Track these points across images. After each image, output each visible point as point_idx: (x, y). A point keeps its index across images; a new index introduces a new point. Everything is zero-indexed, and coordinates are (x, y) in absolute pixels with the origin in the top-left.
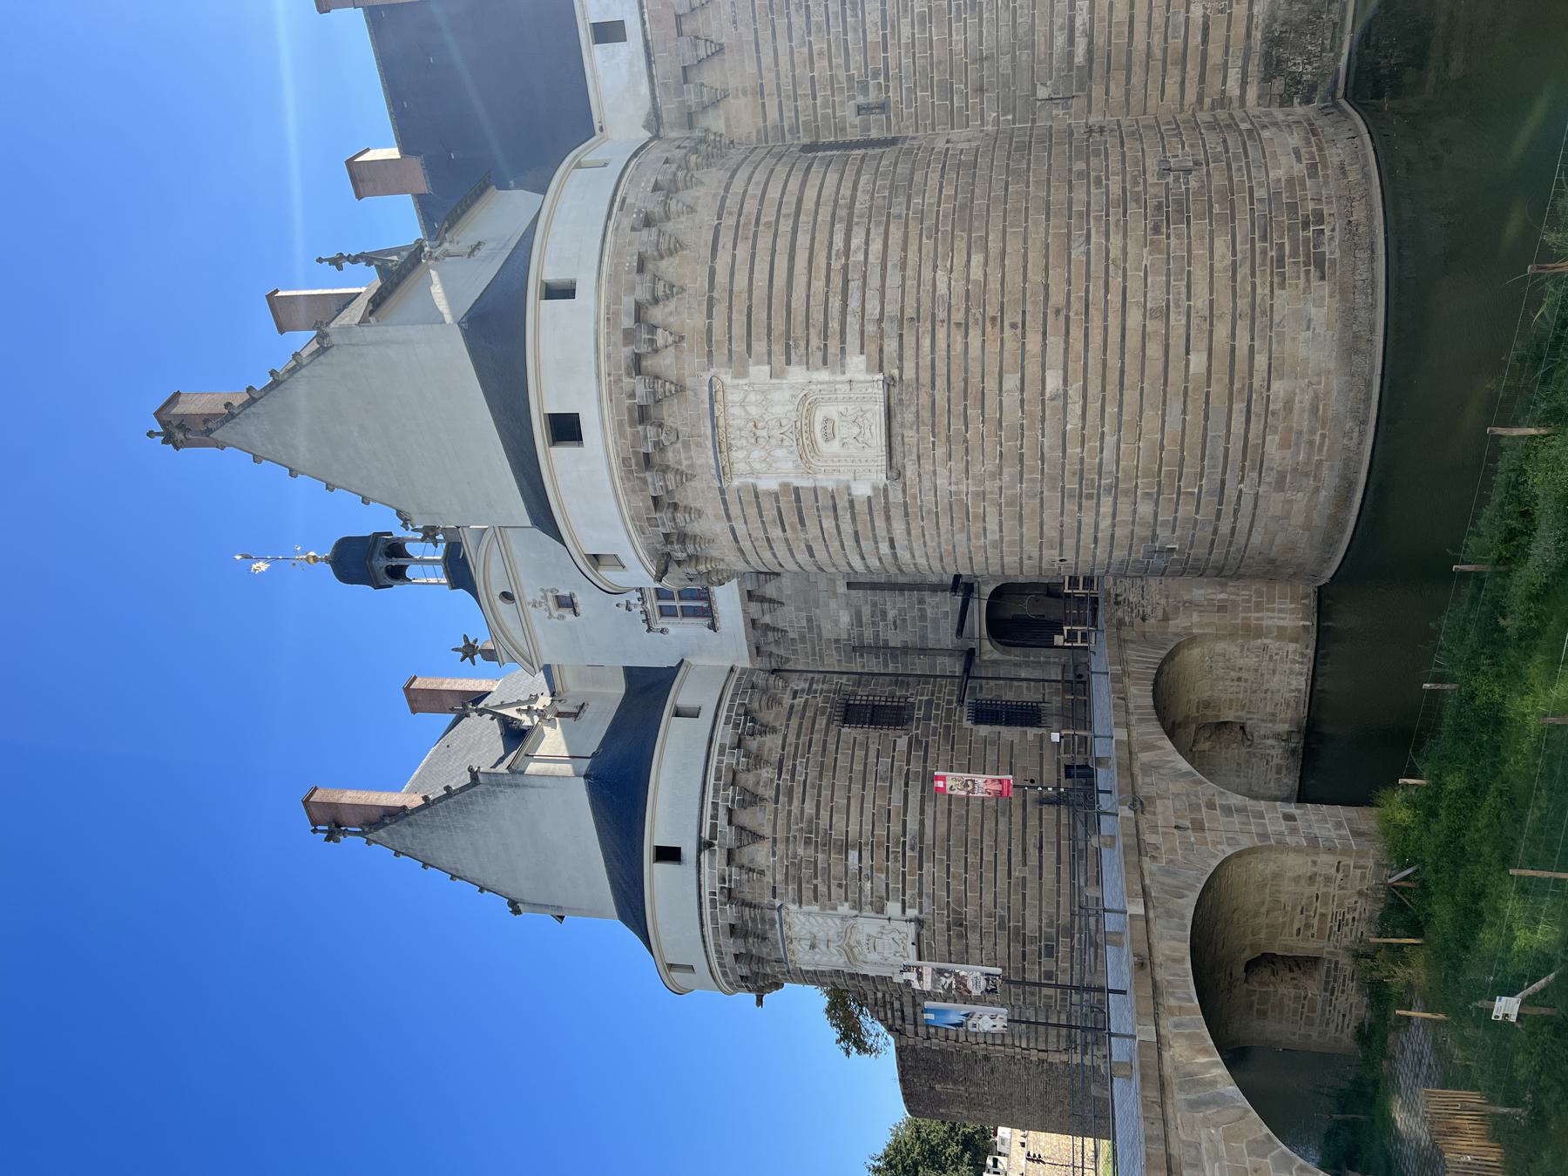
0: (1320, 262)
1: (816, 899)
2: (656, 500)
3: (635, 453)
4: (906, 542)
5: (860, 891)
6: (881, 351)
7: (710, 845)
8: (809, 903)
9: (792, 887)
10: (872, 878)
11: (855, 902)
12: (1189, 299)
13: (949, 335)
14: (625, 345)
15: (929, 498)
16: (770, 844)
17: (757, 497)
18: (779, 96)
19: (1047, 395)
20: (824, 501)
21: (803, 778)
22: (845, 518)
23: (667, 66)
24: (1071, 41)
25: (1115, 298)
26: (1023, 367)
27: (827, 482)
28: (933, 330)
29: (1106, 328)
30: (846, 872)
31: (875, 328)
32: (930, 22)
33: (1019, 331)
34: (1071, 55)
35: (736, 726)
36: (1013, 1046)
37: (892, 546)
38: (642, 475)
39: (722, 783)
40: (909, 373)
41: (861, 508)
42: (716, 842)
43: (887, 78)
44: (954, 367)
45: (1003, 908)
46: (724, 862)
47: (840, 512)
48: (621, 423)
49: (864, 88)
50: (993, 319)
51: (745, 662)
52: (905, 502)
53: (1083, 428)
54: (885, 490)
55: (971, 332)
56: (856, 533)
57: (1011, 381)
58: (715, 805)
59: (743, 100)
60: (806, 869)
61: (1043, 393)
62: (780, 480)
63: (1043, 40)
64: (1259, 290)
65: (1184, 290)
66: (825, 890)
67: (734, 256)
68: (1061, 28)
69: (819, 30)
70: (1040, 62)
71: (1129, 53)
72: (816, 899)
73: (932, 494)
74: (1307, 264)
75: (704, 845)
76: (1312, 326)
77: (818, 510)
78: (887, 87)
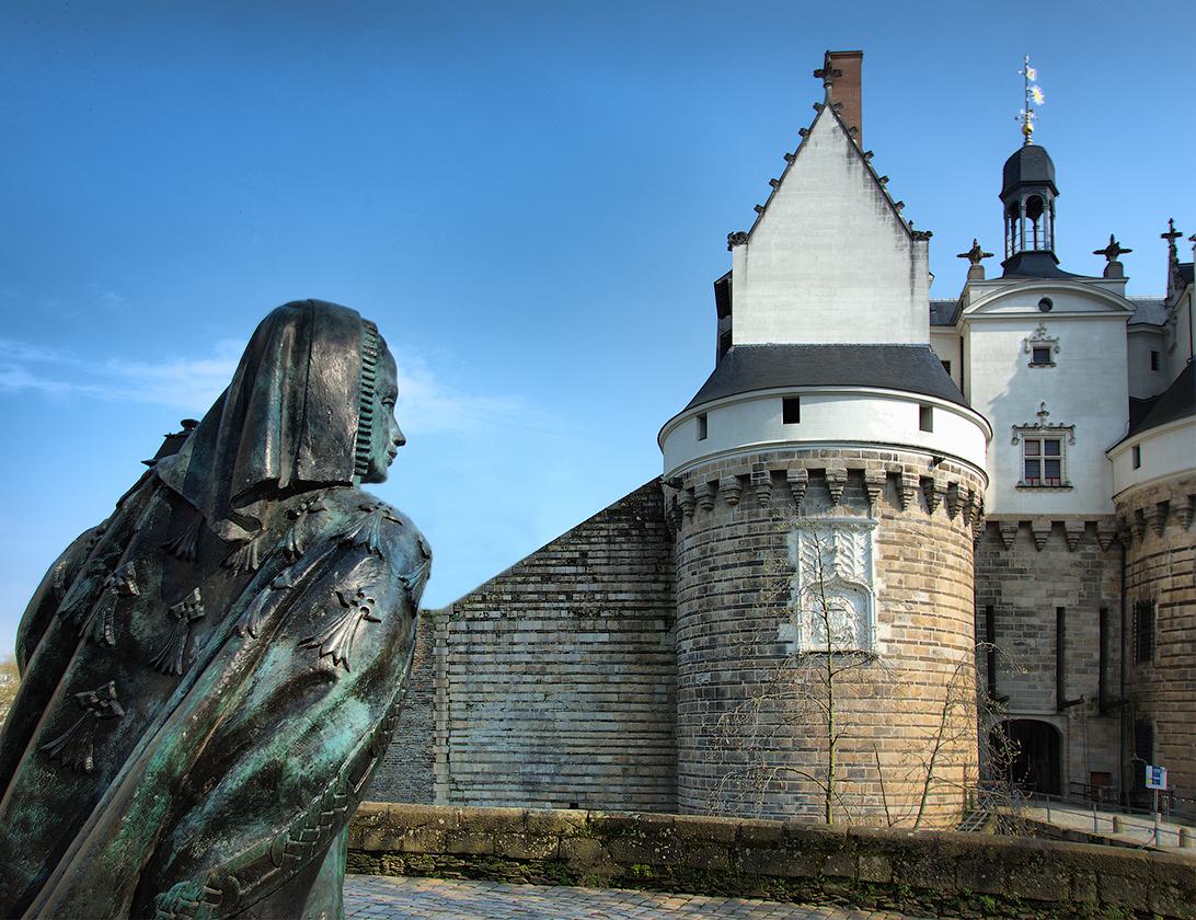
1: (885, 557)
8: (881, 551)
9: (895, 536)
11: (887, 595)
36: (450, 730)
45: (896, 732)
66: (896, 568)
72: (885, 557)
75: (937, 459)
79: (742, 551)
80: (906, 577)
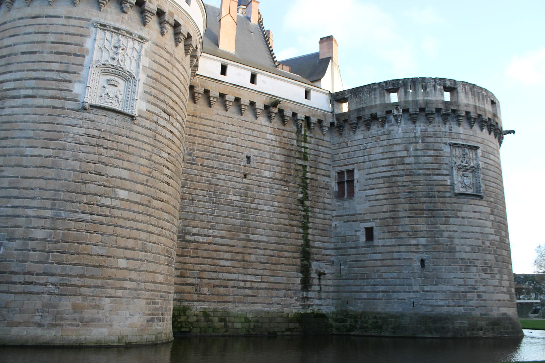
0: (152, 320)
4: (30, 104)
6: (147, 119)
12: (147, 261)
13: (148, 151)
14: (169, 11)
15: (66, 121)
17: (81, 35)
18: (191, 122)
19: (117, 190)
20: (72, 68)
23: (210, 86)
24: (194, 235)
25: (151, 228)
26: (131, 181)
27: (83, 73)
28: (150, 145)
29: (141, 222)
31: (155, 120)
32: (208, 184)
33: (145, 183)
34: (189, 234)
37: (26, 97)
40: (136, 128)
41: (63, 85)
43: (192, 164)
44: (135, 149)
47: (62, 75)
49: (190, 155)
50: (151, 172)
52: (65, 109)
53: (97, 205)
54: (75, 100)
55: (147, 161)
56: (44, 79)
57: (125, 174)
59: (192, 109)
61: (118, 187)
63: (196, 224)
64: (147, 293)
65: (151, 259)
68: (199, 231)
69: (211, 143)
70: (189, 222)
71: (187, 256)
73: (69, 123)
74: (153, 314)
76: (131, 317)
77: (66, 63)
78: (189, 163)
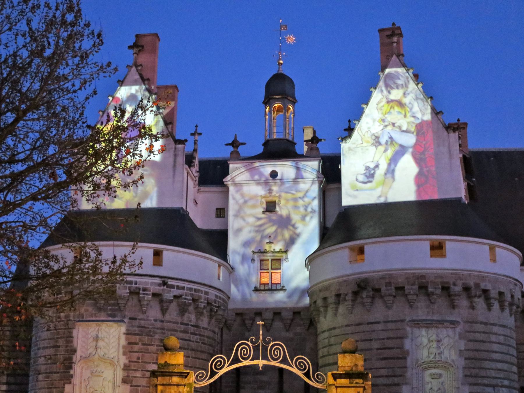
1: (130, 343)
2: (402, 288)
3: (428, 282)
5: (135, 370)
7: (165, 284)
8: (127, 339)
9: (137, 330)
10: (143, 377)
11: (129, 367)
16: (161, 319)
17: (400, 338)
20: (398, 372)
21: (192, 339)
22: (390, 381)
27: (408, 374)
30: (146, 363)
35: (215, 301)
38: (417, 283)
39: (193, 293)
42: (165, 287)
46: (155, 292)
48: (441, 277)
51: (231, 306)
58: (183, 288)
60: (148, 339)
62: (410, 350)
67: (499, 335)
79: (51, 339)
80: (143, 356)
